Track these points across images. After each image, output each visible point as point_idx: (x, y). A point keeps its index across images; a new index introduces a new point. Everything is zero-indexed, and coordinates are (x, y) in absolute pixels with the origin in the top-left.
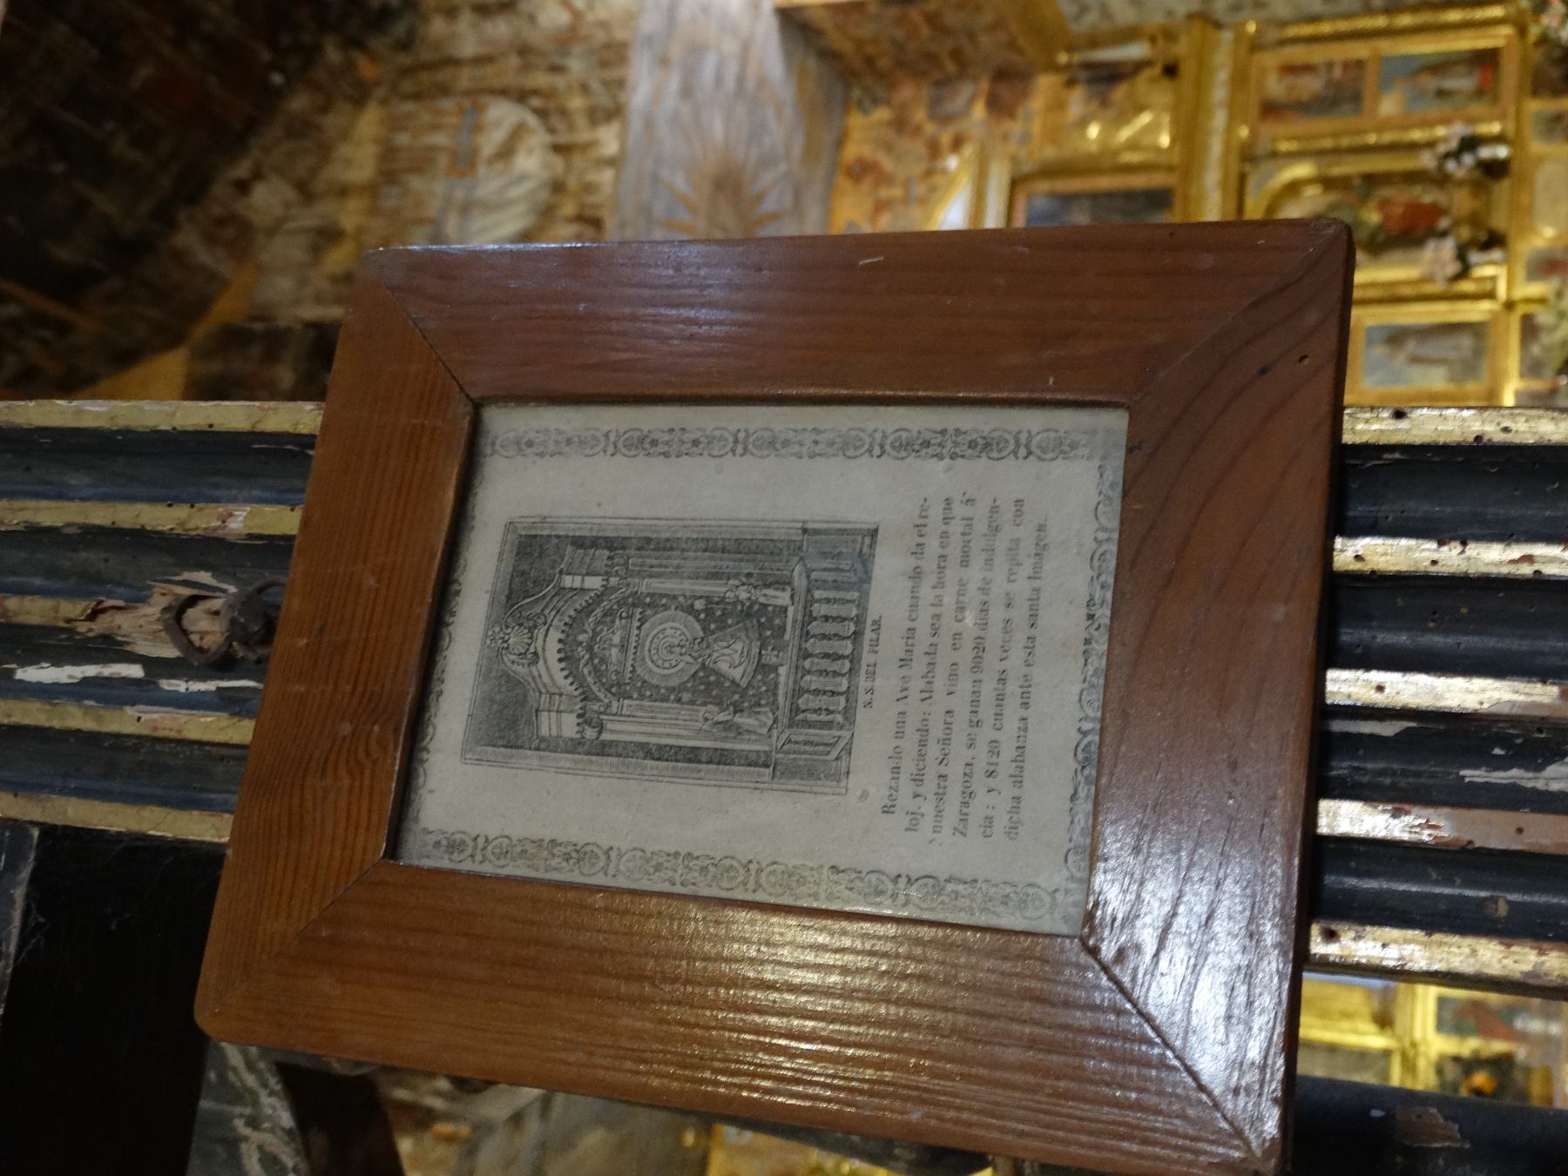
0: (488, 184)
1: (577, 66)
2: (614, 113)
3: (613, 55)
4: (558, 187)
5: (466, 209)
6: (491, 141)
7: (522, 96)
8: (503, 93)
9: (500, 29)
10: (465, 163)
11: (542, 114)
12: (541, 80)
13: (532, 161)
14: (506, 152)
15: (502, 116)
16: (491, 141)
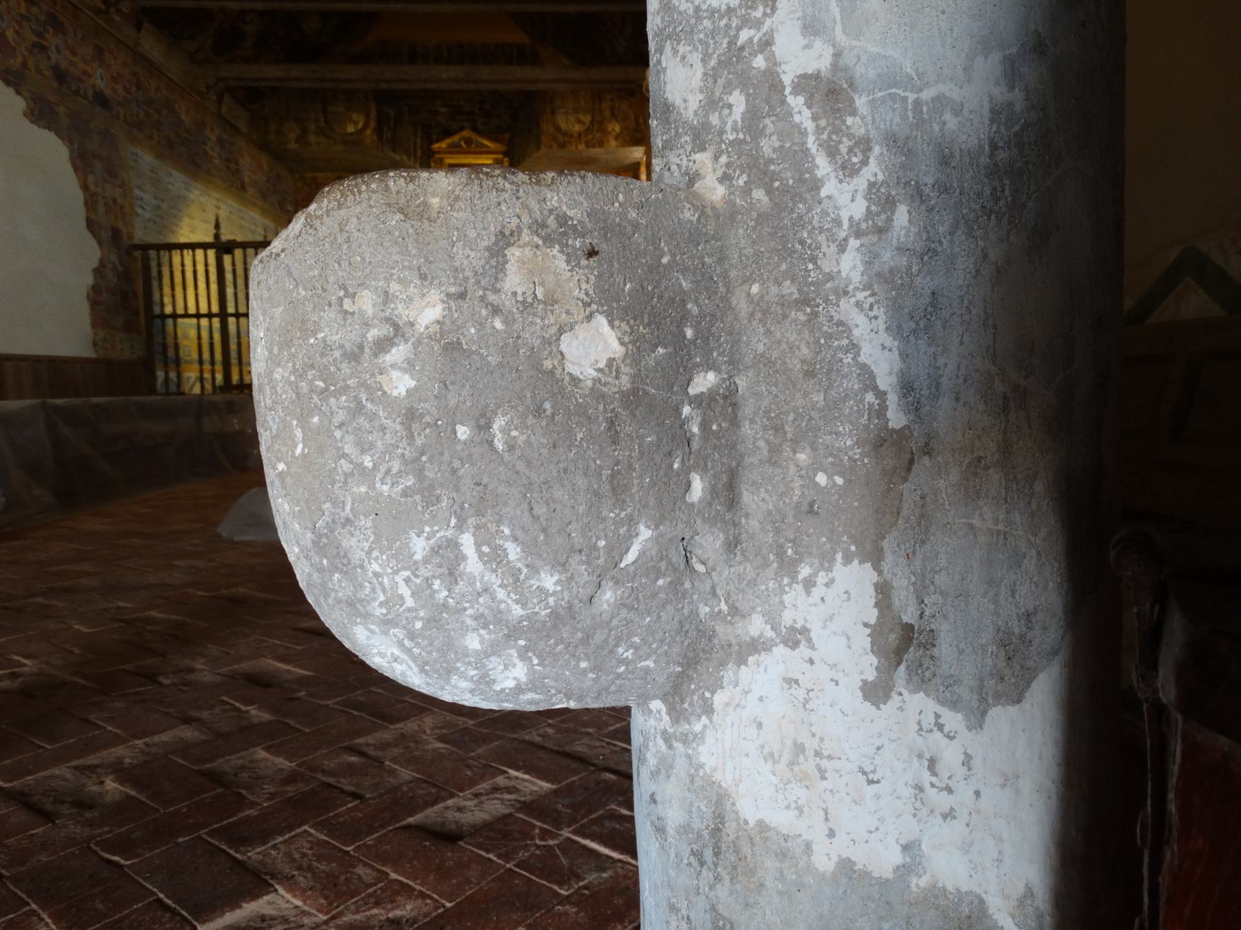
0: (572, 119)
1: (598, 135)
2: (587, 146)
3: (601, 144)
4: (571, 136)
5: (566, 113)
6: (581, 117)
7: (592, 123)
8: (593, 117)
9: (608, 113)
10: (576, 111)
11: (588, 129)
12: (596, 126)
13: (577, 128)
14: (579, 122)
15: (587, 119)
16: (581, 117)
